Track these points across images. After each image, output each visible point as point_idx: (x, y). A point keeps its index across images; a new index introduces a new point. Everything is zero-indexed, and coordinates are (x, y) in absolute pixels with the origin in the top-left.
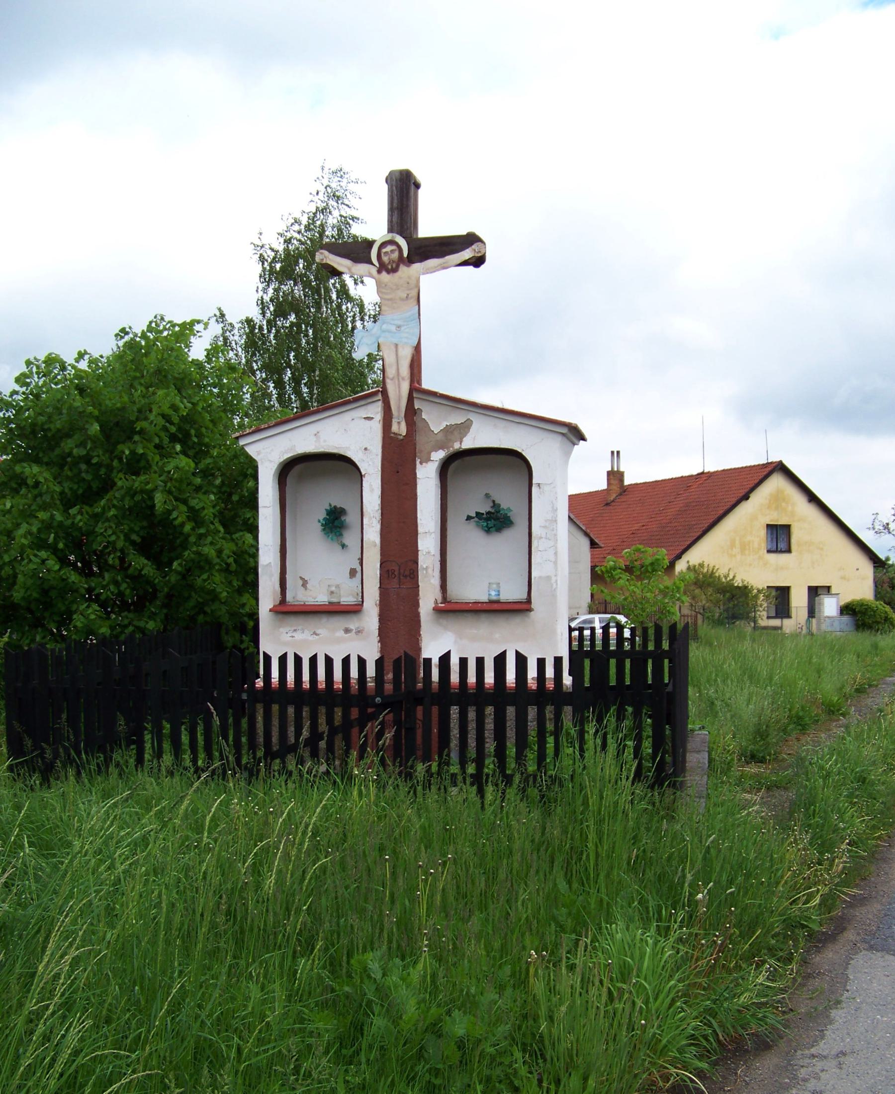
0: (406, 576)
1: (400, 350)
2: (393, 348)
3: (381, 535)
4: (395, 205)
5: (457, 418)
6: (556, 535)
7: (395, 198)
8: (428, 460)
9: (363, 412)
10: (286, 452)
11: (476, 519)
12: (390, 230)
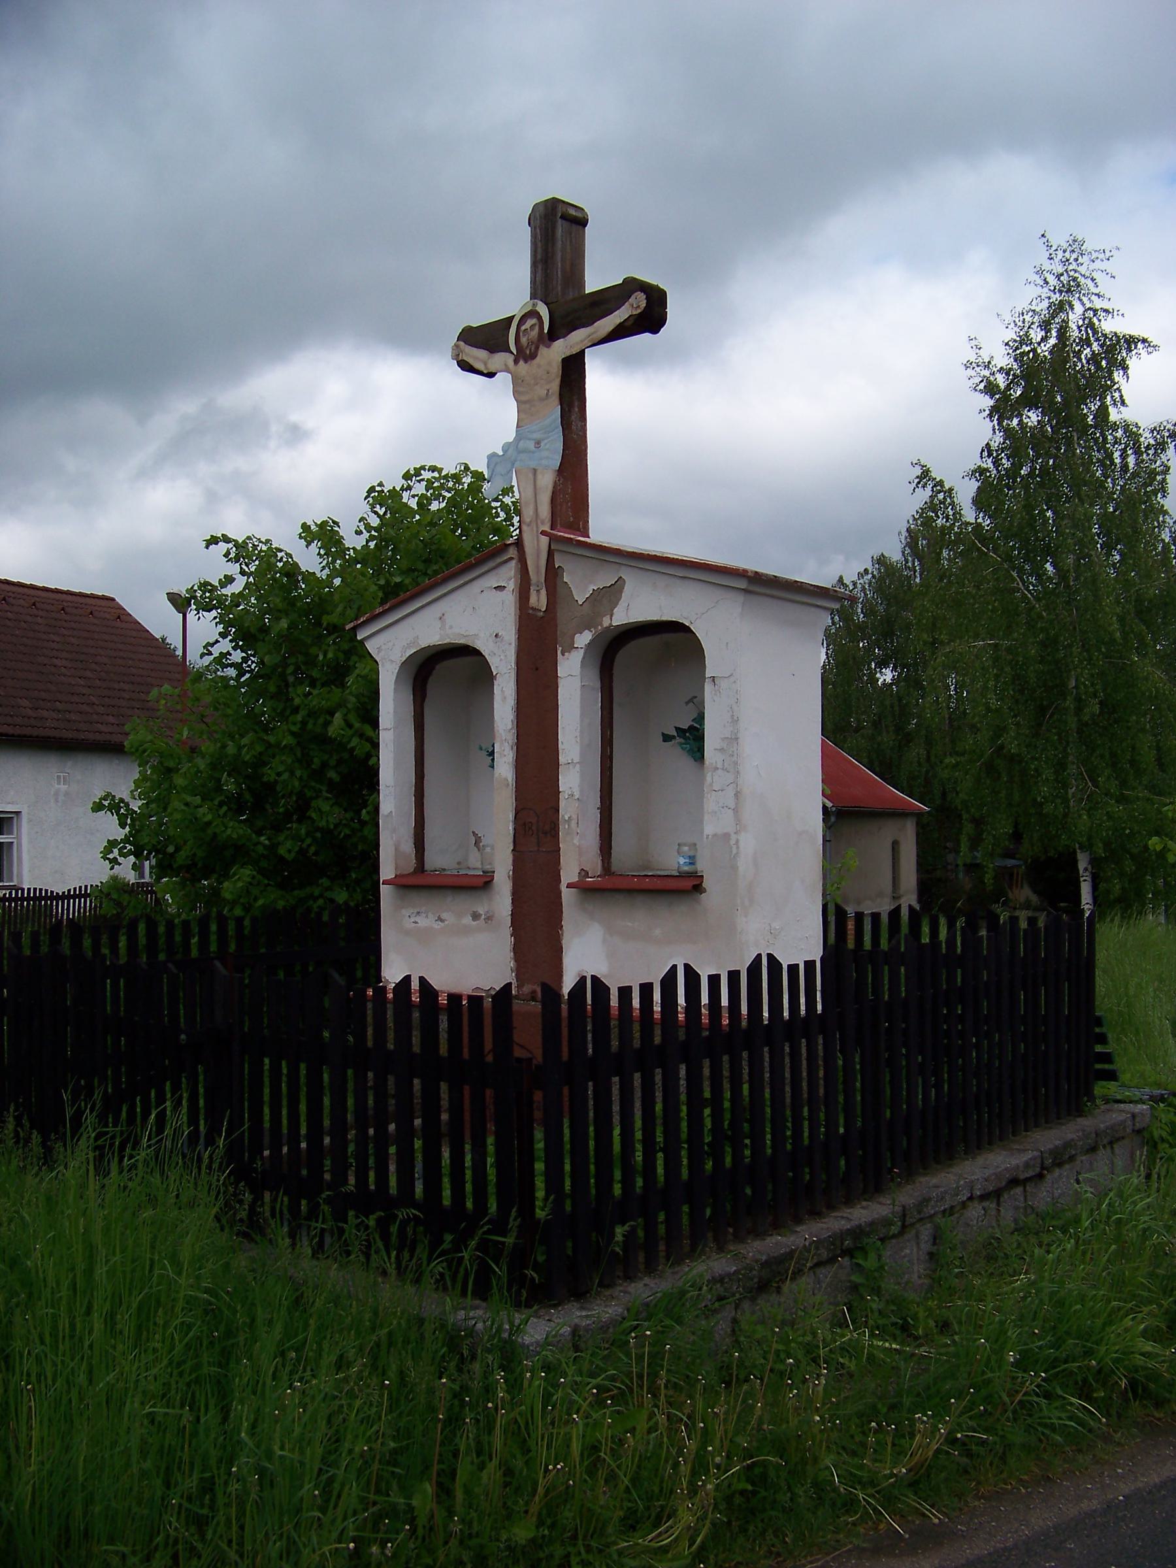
0: (545, 833)
1: (539, 476)
2: (531, 475)
3: (516, 767)
4: (539, 257)
5: (605, 579)
6: (736, 763)
7: (539, 244)
8: (571, 647)
9: (492, 581)
10: (409, 646)
11: (679, 740)
12: (533, 296)
